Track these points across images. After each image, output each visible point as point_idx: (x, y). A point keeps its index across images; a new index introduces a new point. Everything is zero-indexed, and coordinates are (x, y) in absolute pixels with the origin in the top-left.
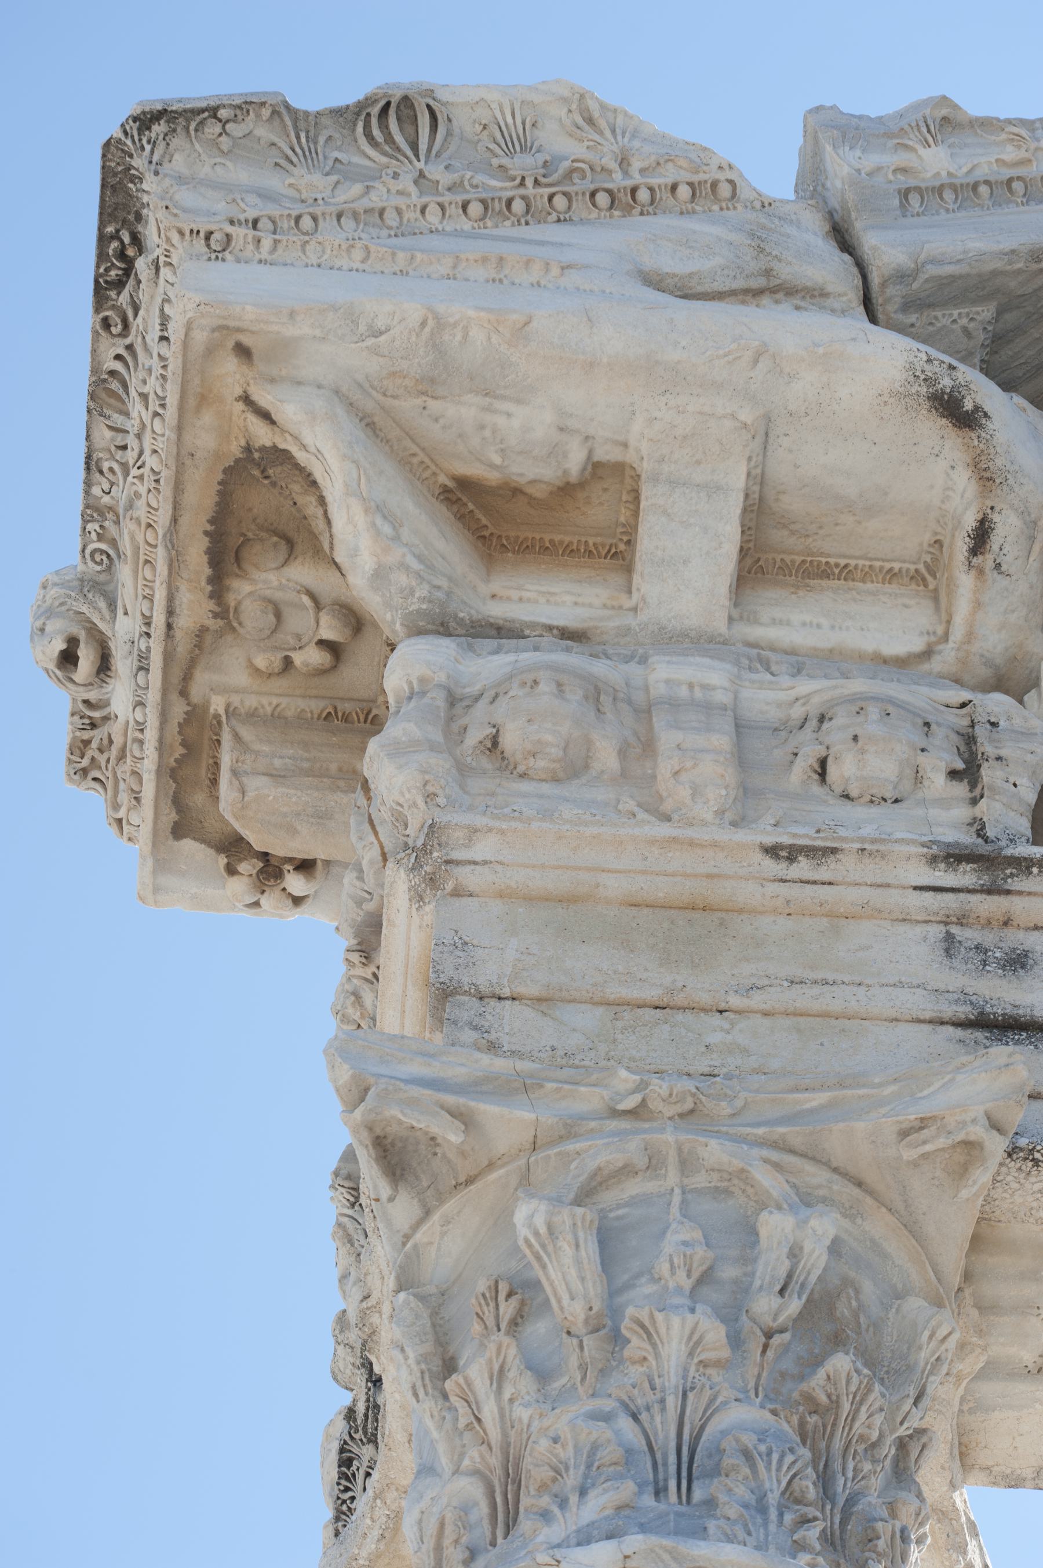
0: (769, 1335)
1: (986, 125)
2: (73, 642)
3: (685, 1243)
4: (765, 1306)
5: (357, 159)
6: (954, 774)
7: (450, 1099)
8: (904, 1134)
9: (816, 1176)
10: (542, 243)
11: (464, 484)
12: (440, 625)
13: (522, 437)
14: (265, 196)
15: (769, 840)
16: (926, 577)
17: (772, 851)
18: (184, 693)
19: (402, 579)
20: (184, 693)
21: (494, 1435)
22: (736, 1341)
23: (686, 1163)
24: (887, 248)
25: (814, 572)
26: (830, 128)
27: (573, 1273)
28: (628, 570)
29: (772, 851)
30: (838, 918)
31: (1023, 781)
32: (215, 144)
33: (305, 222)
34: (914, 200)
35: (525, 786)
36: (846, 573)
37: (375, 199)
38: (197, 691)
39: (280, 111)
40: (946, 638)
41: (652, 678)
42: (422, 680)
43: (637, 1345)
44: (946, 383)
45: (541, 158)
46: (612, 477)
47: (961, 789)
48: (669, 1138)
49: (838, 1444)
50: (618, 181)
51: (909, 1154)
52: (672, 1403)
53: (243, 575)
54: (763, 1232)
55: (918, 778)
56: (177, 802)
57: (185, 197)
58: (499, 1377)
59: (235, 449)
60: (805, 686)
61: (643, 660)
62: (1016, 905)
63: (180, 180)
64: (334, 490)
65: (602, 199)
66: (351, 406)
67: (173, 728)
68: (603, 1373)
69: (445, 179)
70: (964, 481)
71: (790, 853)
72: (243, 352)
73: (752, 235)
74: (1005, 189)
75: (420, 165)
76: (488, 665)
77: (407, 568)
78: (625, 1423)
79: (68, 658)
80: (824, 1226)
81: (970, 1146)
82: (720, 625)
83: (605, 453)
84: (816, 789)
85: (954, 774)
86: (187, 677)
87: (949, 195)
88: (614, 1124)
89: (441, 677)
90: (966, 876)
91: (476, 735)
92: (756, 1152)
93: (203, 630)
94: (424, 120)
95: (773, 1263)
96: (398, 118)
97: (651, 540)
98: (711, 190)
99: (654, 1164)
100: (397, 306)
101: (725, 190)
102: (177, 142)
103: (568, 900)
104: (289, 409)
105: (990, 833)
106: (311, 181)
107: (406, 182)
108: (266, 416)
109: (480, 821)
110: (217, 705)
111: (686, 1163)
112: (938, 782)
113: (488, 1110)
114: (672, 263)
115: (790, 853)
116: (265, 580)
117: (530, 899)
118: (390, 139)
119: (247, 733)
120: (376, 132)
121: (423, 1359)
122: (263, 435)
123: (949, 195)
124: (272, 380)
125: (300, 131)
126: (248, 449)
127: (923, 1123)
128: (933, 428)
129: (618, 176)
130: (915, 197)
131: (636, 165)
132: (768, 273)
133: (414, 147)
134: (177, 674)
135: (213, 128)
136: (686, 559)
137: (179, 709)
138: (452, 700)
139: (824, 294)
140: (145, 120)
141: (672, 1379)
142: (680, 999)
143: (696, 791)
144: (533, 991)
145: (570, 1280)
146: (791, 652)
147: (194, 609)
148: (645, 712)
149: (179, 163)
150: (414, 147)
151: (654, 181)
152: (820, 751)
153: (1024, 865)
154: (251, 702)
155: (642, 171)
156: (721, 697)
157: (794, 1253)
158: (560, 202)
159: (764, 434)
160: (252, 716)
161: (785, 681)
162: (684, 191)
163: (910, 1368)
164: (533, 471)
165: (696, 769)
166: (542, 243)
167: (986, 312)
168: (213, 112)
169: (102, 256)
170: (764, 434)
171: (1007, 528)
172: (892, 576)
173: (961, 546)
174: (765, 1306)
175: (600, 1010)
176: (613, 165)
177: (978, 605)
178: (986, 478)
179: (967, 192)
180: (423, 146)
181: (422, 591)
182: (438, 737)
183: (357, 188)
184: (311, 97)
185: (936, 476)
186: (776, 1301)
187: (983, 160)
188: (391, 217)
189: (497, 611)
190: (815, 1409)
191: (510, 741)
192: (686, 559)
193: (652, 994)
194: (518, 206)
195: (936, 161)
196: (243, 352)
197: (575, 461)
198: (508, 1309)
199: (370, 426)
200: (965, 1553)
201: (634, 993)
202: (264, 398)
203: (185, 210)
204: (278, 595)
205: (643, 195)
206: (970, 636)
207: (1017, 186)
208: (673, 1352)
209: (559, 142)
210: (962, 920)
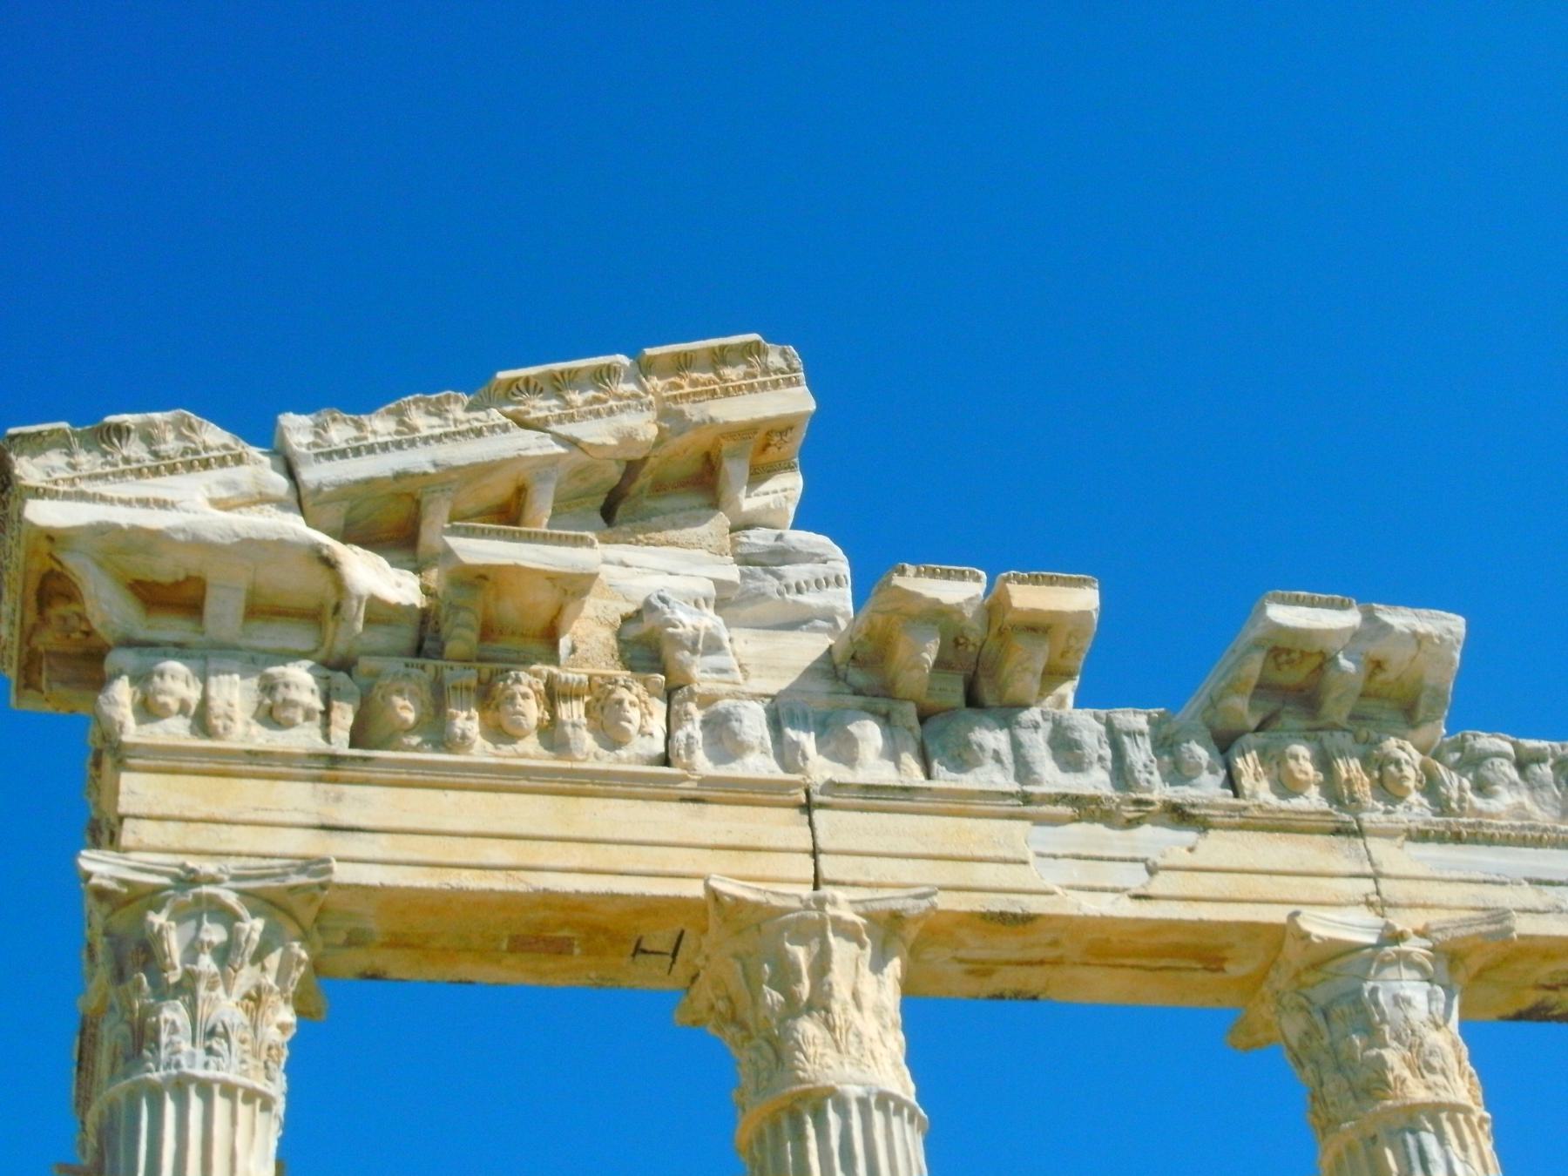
20: (28, 643)
56: (26, 677)
59: (46, 569)
83: (194, 573)
97: (210, 608)
108: (59, 562)
110: (41, 648)
116: (59, 609)
122: (57, 568)
135: (39, 440)
137: (26, 649)
146: (264, 652)
147: (31, 617)
160: (55, 655)
164: (166, 579)
173: (329, 611)
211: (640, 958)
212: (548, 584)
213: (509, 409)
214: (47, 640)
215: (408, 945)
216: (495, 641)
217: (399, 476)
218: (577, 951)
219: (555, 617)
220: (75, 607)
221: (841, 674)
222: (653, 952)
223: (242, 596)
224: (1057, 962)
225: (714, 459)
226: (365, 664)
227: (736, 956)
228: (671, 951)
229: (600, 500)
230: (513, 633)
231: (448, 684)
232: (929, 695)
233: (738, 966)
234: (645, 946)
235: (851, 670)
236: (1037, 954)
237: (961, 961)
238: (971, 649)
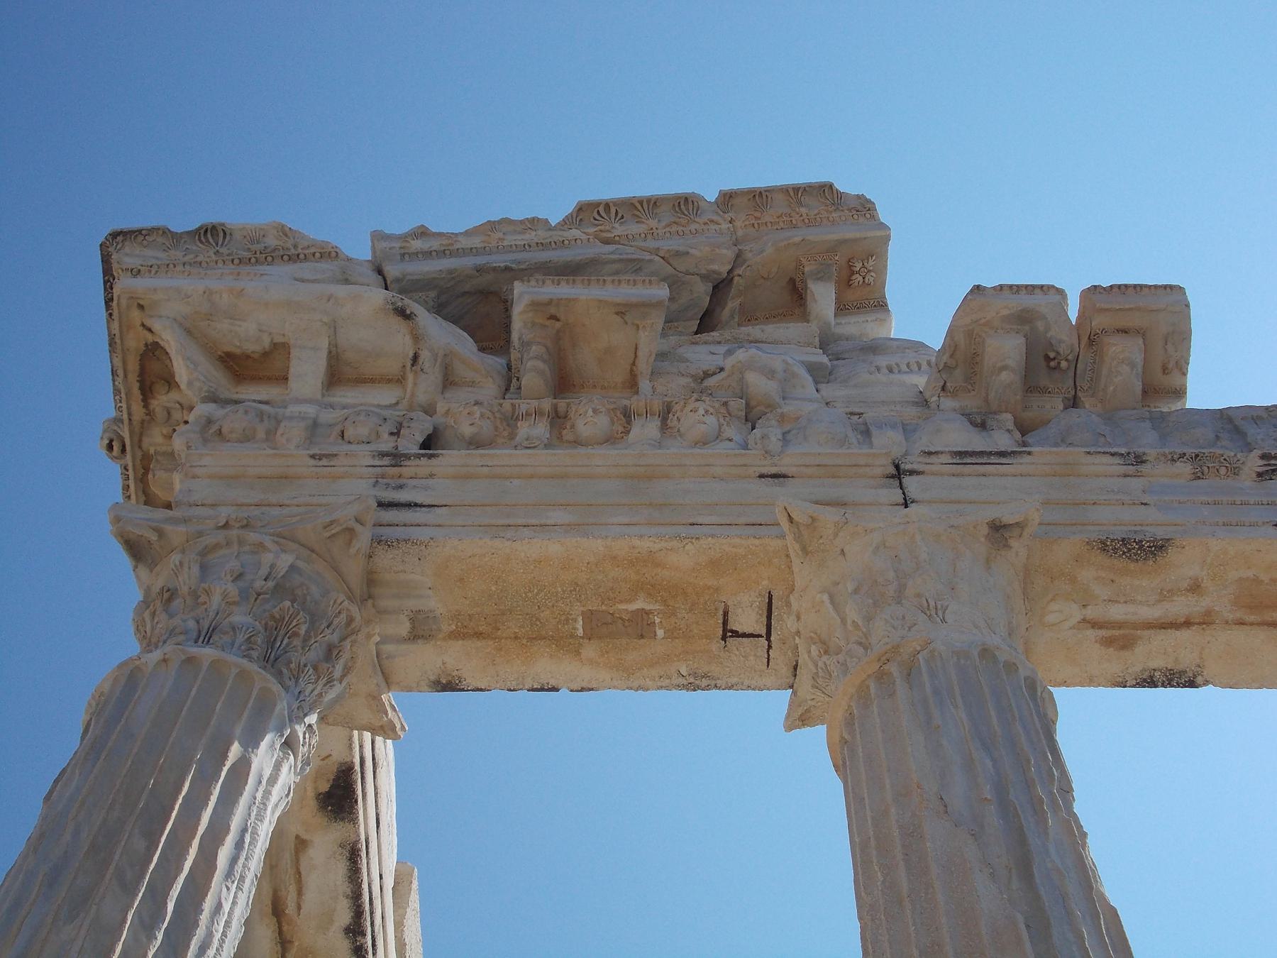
0: (259, 594)
1: (440, 235)
2: (111, 441)
4: (259, 584)
6: (392, 434)
7: (154, 524)
11: (229, 355)
12: (213, 398)
13: (246, 334)
14: (157, 258)
15: (311, 452)
16: (400, 380)
17: (313, 457)
19: (197, 384)
20: (140, 447)
23: (241, 542)
24: (392, 271)
25: (362, 381)
26: (377, 236)
29: (313, 457)
31: (417, 434)
32: (141, 243)
33: (169, 266)
34: (407, 257)
36: (372, 381)
37: (199, 259)
38: (145, 445)
39: (165, 232)
44: (400, 304)
46: (279, 350)
51: (328, 534)
53: (154, 398)
55: (378, 435)
57: (127, 259)
62: (404, 470)
64: (173, 353)
65: (286, 258)
66: (181, 325)
67: (138, 462)
70: (408, 340)
71: (320, 457)
72: (141, 307)
74: (442, 253)
79: (110, 447)
81: (350, 531)
82: (319, 396)
85: (392, 434)
86: (140, 441)
90: (386, 461)
93: (143, 422)
94: (221, 234)
95: (264, 571)
96: (211, 233)
98: (327, 254)
99: (228, 544)
100: (193, 285)
101: (333, 254)
102: (127, 243)
104: (157, 326)
107: (211, 253)
108: (150, 330)
110: (152, 451)
113: (168, 528)
115: (320, 457)
116: (162, 400)
118: (208, 241)
122: (150, 338)
125: (172, 238)
126: (146, 345)
127: (332, 523)
128: (397, 322)
134: (136, 439)
135: (140, 238)
136: (307, 372)
137: (139, 454)
140: (114, 235)
141: (215, 607)
143: (288, 440)
147: (138, 411)
149: (127, 250)
153: (408, 457)
157: (272, 566)
158: (269, 259)
159: (334, 327)
162: (318, 255)
164: (250, 347)
167: (433, 294)
170: (334, 327)
171: (425, 355)
172: (389, 381)
177: (415, 384)
178: (416, 338)
179: (428, 254)
181: (205, 388)
183: (192, 256)
184: (177, 227)
185: (399, 341)
187: (435, 244)
188: (204, 265)
189: (235, 397)
191: (224, 430)
192: (307, 372)
194: (253, 260)
195: (417, 245)
196: (141, 307)
197: (266, 342)
198: (166, 595)
199: (189, 332)
200: (387, 714)
202: (148, 323)
204: (168, 405)
205: (302, 256)
206: (413, 395)
208: (216, 599)
209: (272, 241)
211: (732, 642)
212: (618, 319)
213: (592, 230)
215: (479, 635)
217: (480, 270)
218: (660, 633)
219: (634, 364)
222: (744, 635)
224: (1206, 621)
225: (799, 285)
228: (764, 632)
234: (734, 625)
236: (1179, 607)
237: (1095, 625)
238: (1064, 364)
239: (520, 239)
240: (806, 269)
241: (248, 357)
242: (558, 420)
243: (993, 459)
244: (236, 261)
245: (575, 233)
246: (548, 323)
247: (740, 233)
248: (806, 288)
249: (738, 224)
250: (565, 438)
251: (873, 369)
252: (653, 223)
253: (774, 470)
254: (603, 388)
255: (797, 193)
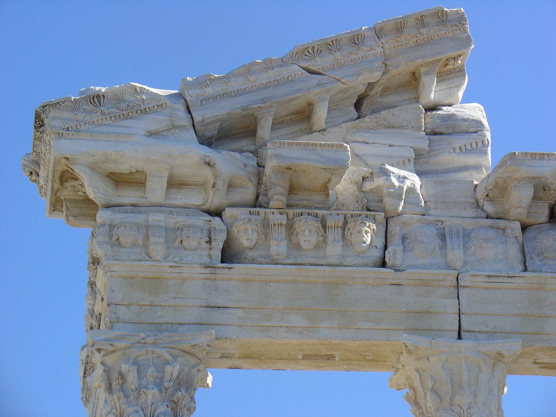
0: (167, 390)
3: (152, 372)
5: (88, 108)
6: (207, 242)
7: (110, 343)
8: (192, 346)
9: (176, 352)
10: (126, 127)
11: (111, 173)
18: (55, 195)
20: (55, 195)
21: (118, 409)
22: (161, 391)
23: (153, 353)
24: (198, 117)
27: (132, 379)
28: (145, 186)
30: (183, 280)
32: (59, 108)
34: (204, 101)
35: (124, 250)
40: (207, 201)
41: (149, 219)
42: (104, 222)
43: (143, 395)
45: (126, 103)
47: (208, 245)
48: (150, 349)
49: (179, 409)
50: (143, 107)
52: (149, 408)
54: (166, 370)
57: (54, 123)
58: (119, 399)
60: (180, 219)
61: (147, 213)
63: (53, 118)
68: (138, 398)
69: (107, 112)
73: (170, 117)
75: (101, 108)
76: (118, 217)
77: (100, 197)
78: (141, 412)
80: (177, 367)
84: (180, 246)
85: (207, 242)
87: (211, 99)
88: (140, 345)
89: (108, 222)
90: (208, 271)
91: (114, 238)
92: (165, 350)
94: (102, 97)
101: (164, 105)
103: (132, 278)
105: (213, 258)
106: (80, 116)
109: (116, 262)
110: (62, 197)
111: (153, 353)
112: (204, 245)
114: (153, 127)
117: (125, 278)
118: (94, 102)
119: (68, 205)
120: (92, 101)
121: (106, 385)
123: (211, 99)
124: (73, 164)
129: (142, 106)
130: (205, 101)
131: (146, 102)
132: (173, 125)
133: (100, 103)
135: (58, 106)
136: (156, 191)
137: (54, 197)
138: (110, 226)
139: (185, 126)
141: (149, 403)
142: (153, 304)
144: (126, 303)
145: (132, 379)
147: (57, 186)
148: (147, 227)
149: (52, 114)
150: (100, 103)
151: (150, 106)
152: (181, 239)
154: (69, 197)
155: (147, 104)
156: (163, 224)
160: (69, 200)
161: (175, 217)
162: (156, 107)
163: (193, 385)
165: (157, 247)
166: (126, 127)
167: (218, 124)
168: (58, 103)
169: (36, 122)
171: (219, 183)
174: (166, 384)
175: (138, 307)
176: (141, 104)
179: (214, 98)
180: (102, 103)
182: (107, 240)
186: (168, 384)
190: (175, 403)
191: (121, 239)
193: (148, 303)
194: (122, 116)
195: (209, 91)
199: (93, 169)
201: (144, 303)
203: (54, 127)
205: (147, 110)
207: (225, 95)
208: (150, 397)
210: (207, 279)
214: (65, 194)
215: (252, 358)
216: (296, 194)
220: (78, 182)
221: (480, 204)
223: (166, 180)
226: (228, 213)
227: (417, 370)
229: (354, 100)
230: (305, 190)
231: (271, 223)
232: (528, 217)
233: (418, 376)
235: (486, 203)
239: (264, 78)
240: (422, 71)
241: (122, 174)
242: (290, 226)
243: (506, 280)
244: (113, 118)
245: (295, 67)
246: (285, 171)
247: (387, 52)
248: (420, 78)
249: (387, 46)
250: (293, 242)
251: (452, 150)
252: (338, 55)
253: (397, 282)
254: (310, 190)
255: (421, 21)
